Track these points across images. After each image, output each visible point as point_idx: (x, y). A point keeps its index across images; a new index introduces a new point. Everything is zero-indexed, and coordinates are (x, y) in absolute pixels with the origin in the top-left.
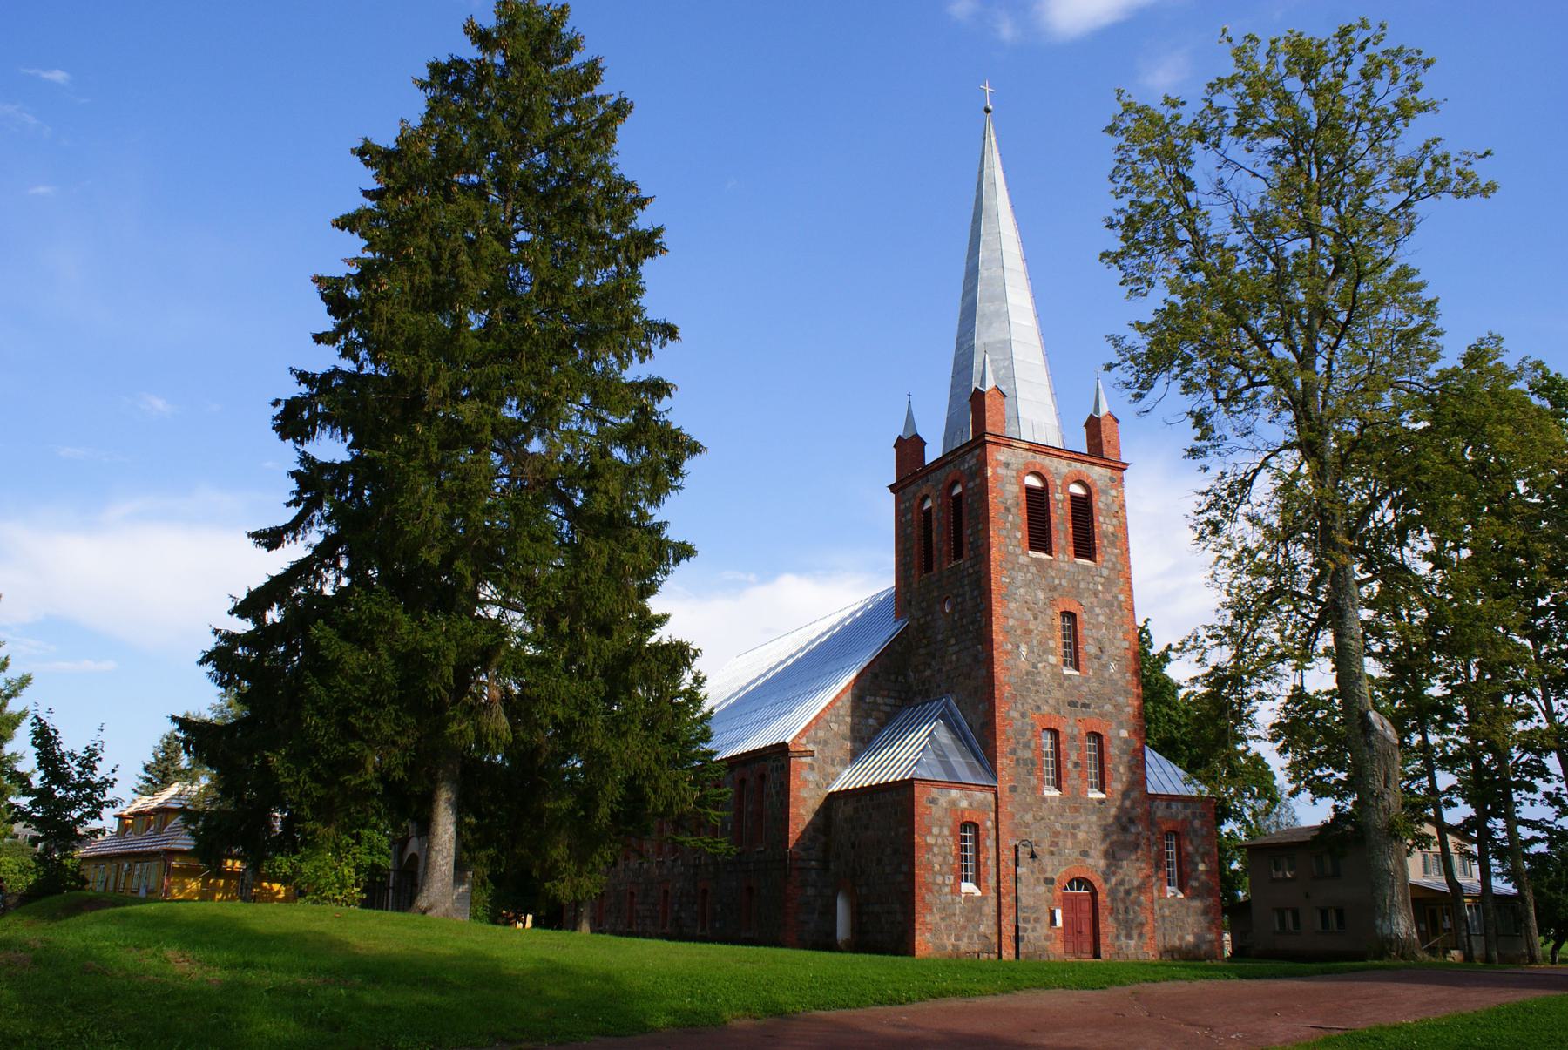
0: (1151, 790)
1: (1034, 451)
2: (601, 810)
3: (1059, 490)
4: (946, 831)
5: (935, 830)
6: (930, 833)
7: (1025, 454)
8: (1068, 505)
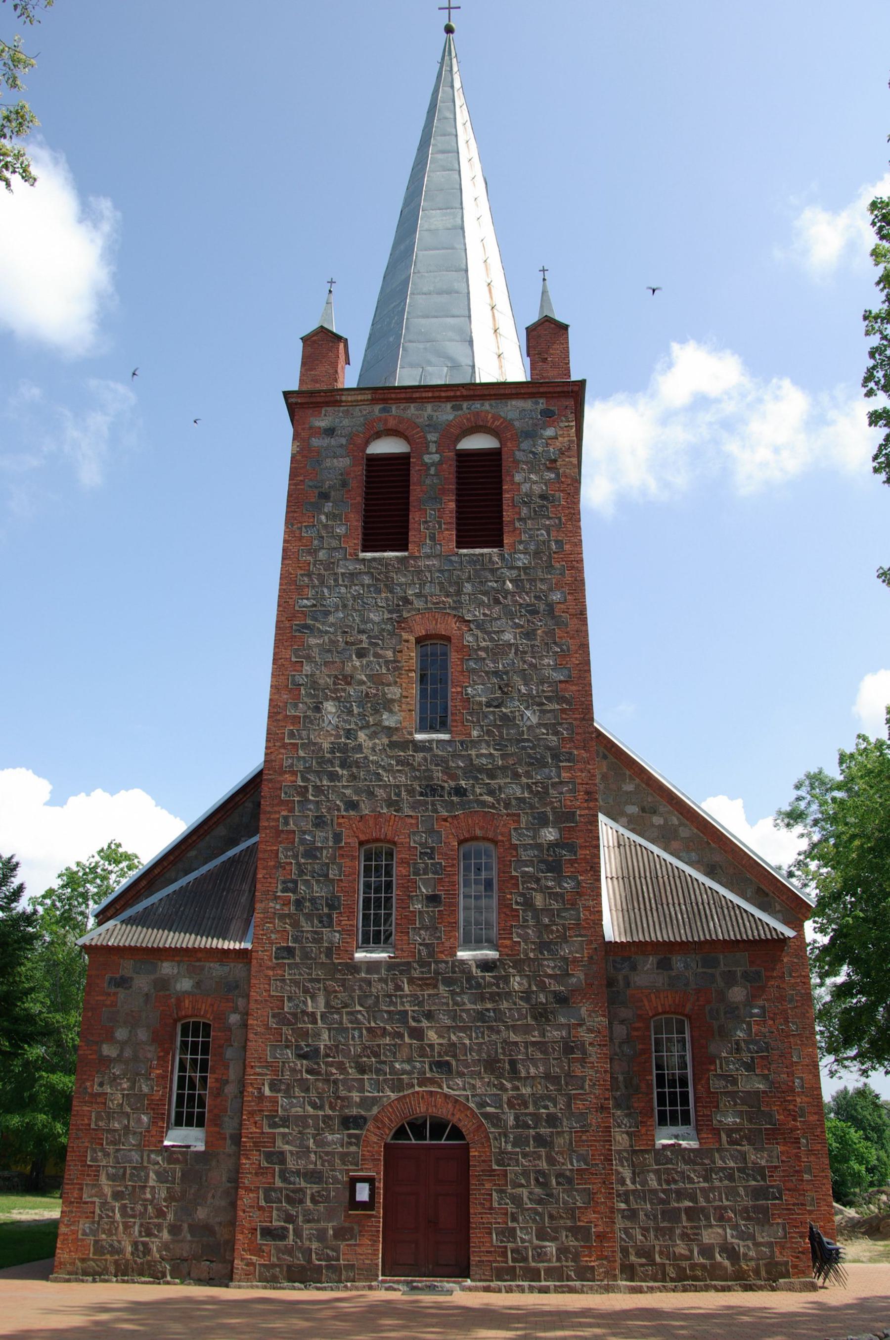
0: (607, 939)
1: (384, 400)
2: (217, 965)
3: (433, 448)
4: (143, 1035)
5: (121, 1034)
6: (110, 1038)
7: (366, 409)
8: (450, 471)
